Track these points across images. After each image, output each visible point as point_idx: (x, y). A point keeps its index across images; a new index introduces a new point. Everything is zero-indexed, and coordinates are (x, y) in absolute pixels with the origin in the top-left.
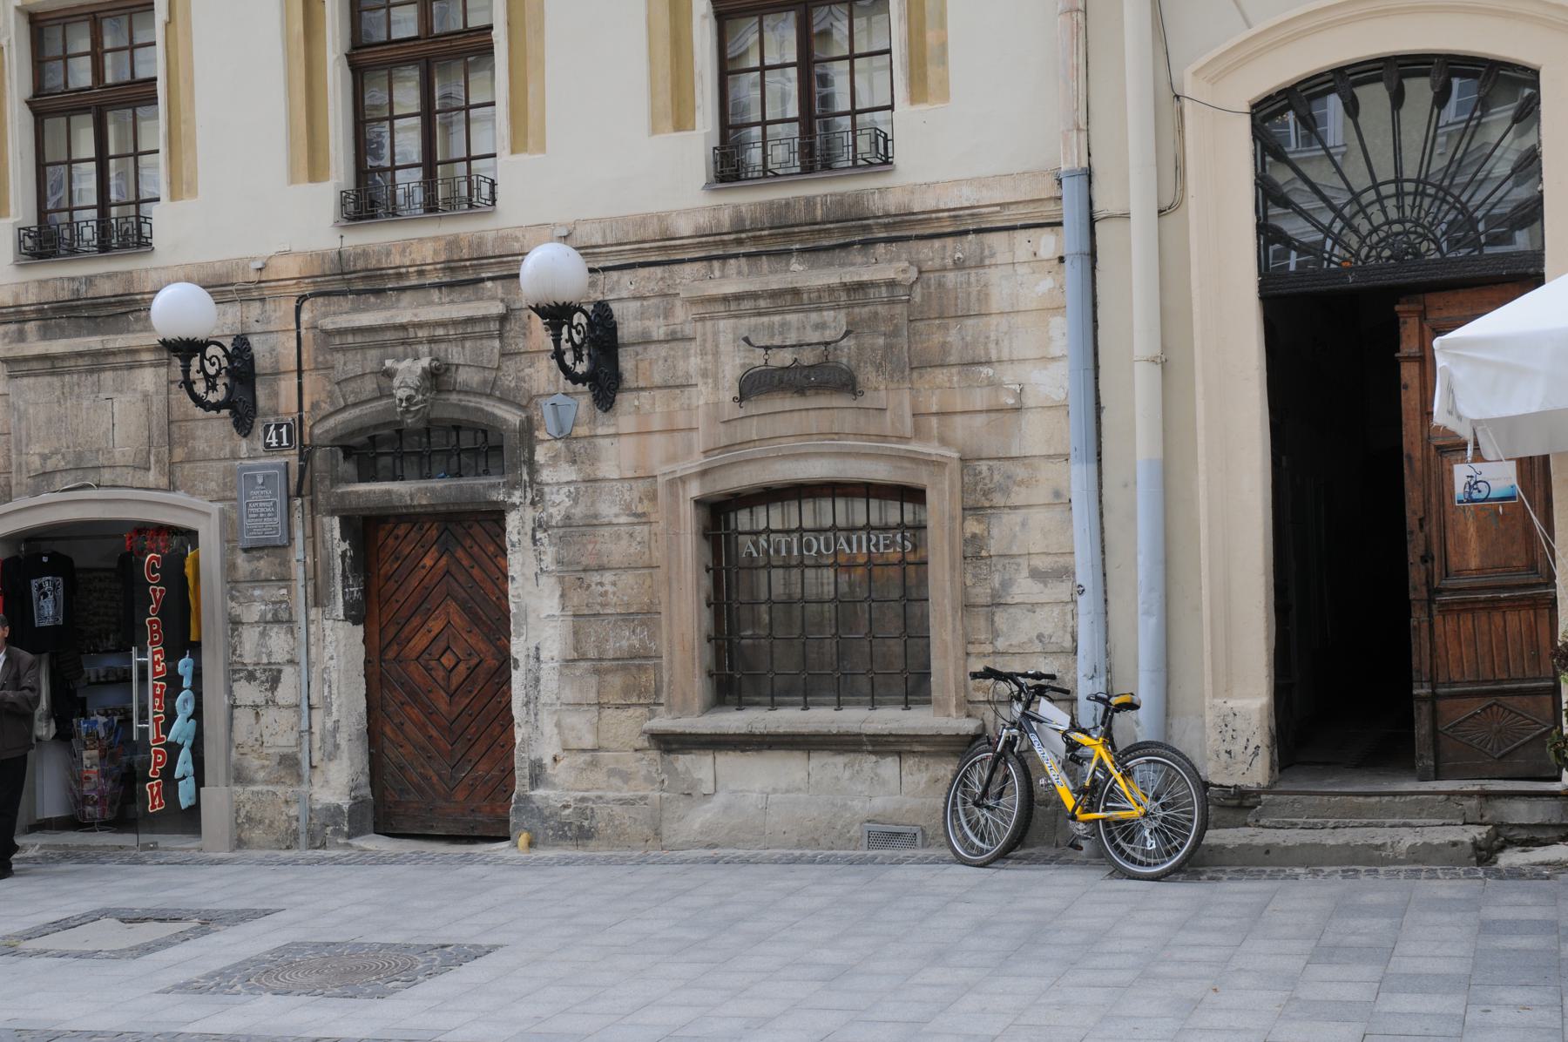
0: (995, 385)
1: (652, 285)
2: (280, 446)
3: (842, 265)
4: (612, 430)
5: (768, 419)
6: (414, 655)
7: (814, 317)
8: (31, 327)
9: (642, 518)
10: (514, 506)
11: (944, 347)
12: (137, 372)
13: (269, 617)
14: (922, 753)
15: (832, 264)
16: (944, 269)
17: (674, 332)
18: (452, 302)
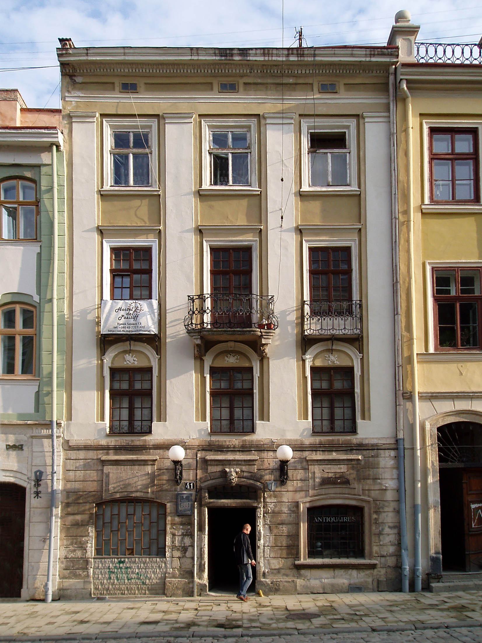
0: (381, 484)
1: (297, 455)
4: (286, 490)
5: (327, 489)
7: (339, 466)
8: (110, 451)
11: (369, 475)
12: (146, 467)
14: (362, 569)
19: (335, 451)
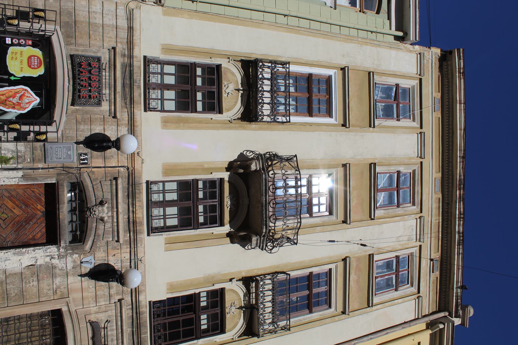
2: (80, 160)
3: (129, 343)
6: (5, 203)
7: (115, 338)
9: (55, 292)
10: (59, 250)
13: (19, 154)
15: (129, 340)
17: (112, 296)
18: (124, 223)
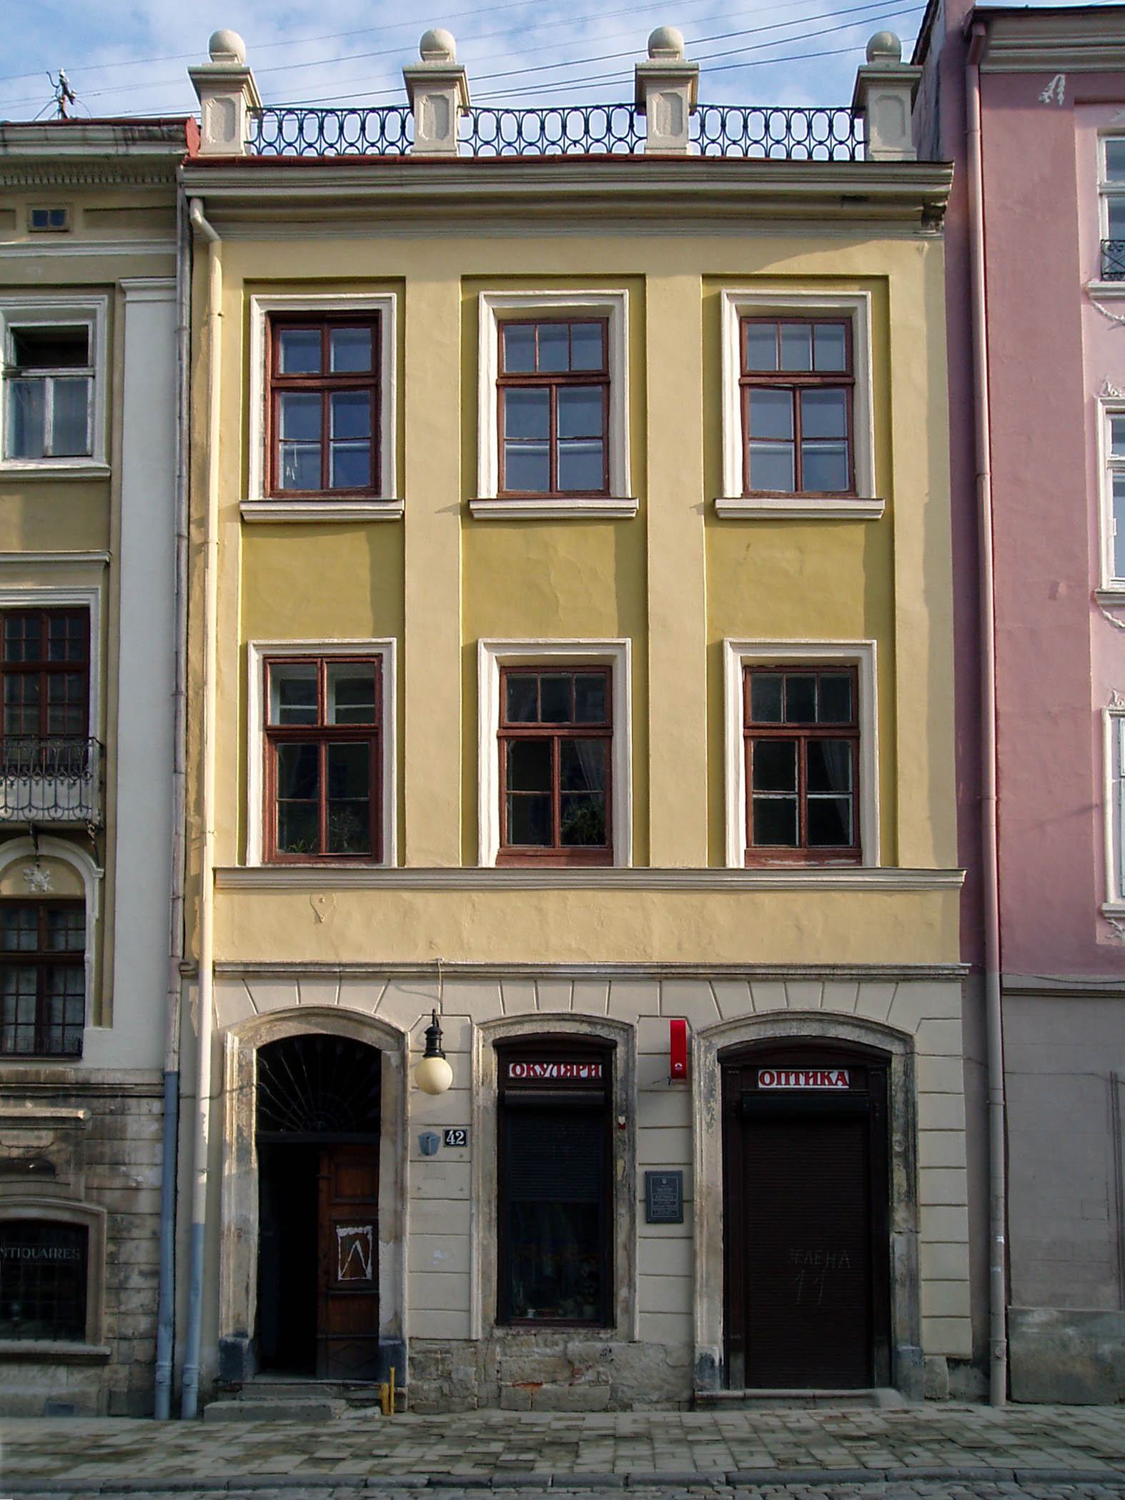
0: (126, 1176)
7: (36, 1133)
11: (102, 1154)
14: (79, 1364)
16: (104, 1114)
19: (32, 1098)
